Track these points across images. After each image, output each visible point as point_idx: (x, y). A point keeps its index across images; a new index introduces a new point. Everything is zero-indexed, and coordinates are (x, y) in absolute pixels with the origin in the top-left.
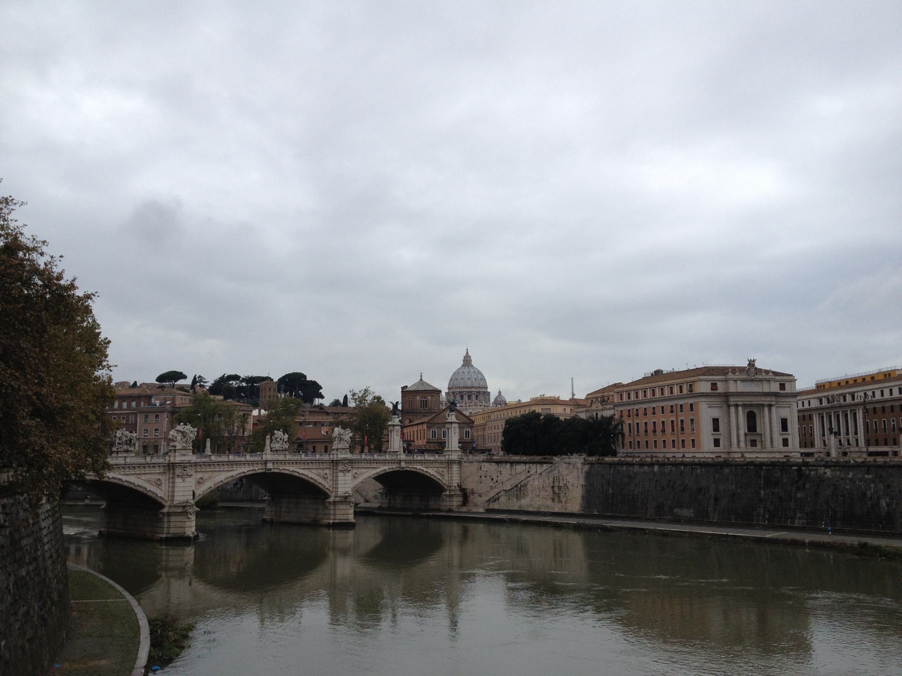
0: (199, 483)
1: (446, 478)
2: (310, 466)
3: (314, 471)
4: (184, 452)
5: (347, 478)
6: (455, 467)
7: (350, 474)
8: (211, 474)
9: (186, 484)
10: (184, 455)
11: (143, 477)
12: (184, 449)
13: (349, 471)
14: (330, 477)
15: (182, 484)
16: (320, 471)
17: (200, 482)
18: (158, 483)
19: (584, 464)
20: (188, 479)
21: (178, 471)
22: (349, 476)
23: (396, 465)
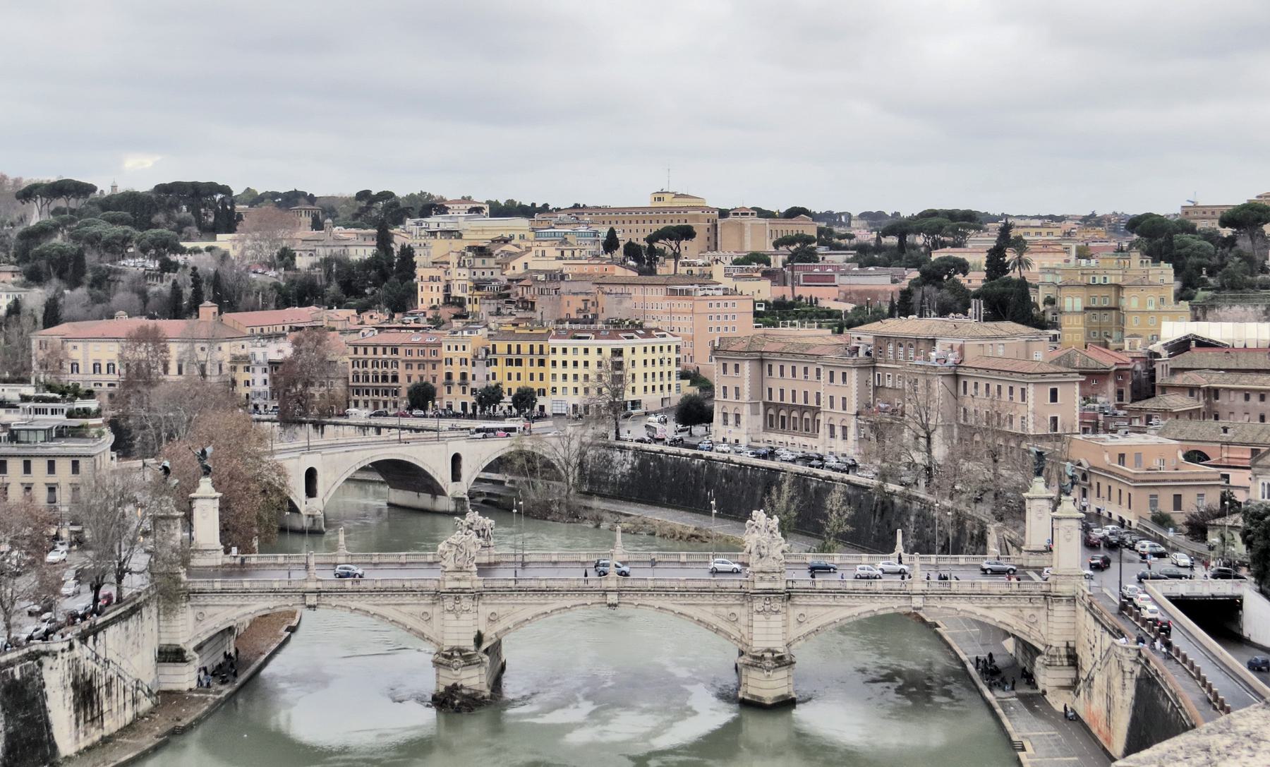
0: (490, 620)
1: (1043, 630)
2: (699, 600)
3: (710, 609)
4: (458, 575)
5: (772, 624)
6: (1061, 610)
7: (779, 617)
8: (510, 607)
9: (461, 623)
10: (458, 580)
11: (403, 609)
12: (460, 570)
13: (777, 612)
14: (744, 620)
15: (455, 623)
16: (723, 610)
17: (493, 619)
18: (427, 618)
19: (1136, 662)
20: (464, 616)
21: (449, 603)
22: (776, 621)
23: (903, 602)
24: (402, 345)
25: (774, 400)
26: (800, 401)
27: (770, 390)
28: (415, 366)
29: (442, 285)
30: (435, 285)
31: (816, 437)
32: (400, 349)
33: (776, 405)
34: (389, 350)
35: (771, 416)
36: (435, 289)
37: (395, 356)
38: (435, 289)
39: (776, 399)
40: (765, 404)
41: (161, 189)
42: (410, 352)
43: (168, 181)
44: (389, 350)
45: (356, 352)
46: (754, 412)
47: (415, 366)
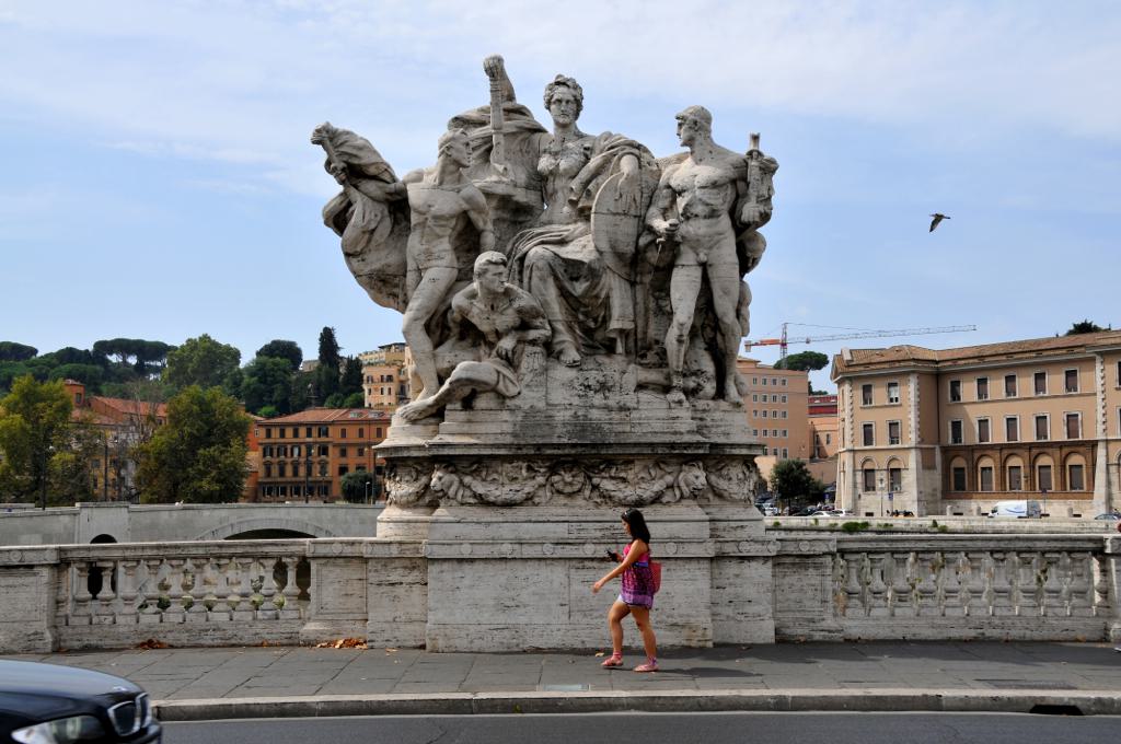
24: (333, 423)
25: (965, 440)
26: (1027, 435)
27: (957, 426)
28: (352, 452)
29: (394, 386)
30: (386, 387)
31: (1090, 494)
32: (331, 430)
33: (972, 449)
34: (315, 431)
35: (959, 470)
36: (386, 392)
37: (323, 439)
38: (386, 392)
39: (970, 437)
40: (945, 450)
41: (104, 347)
42: (344, 433)
43: (109, 337)
44: (315, 431)
45: (269, 435)
46: (926, 465)
47: (352, 452)
